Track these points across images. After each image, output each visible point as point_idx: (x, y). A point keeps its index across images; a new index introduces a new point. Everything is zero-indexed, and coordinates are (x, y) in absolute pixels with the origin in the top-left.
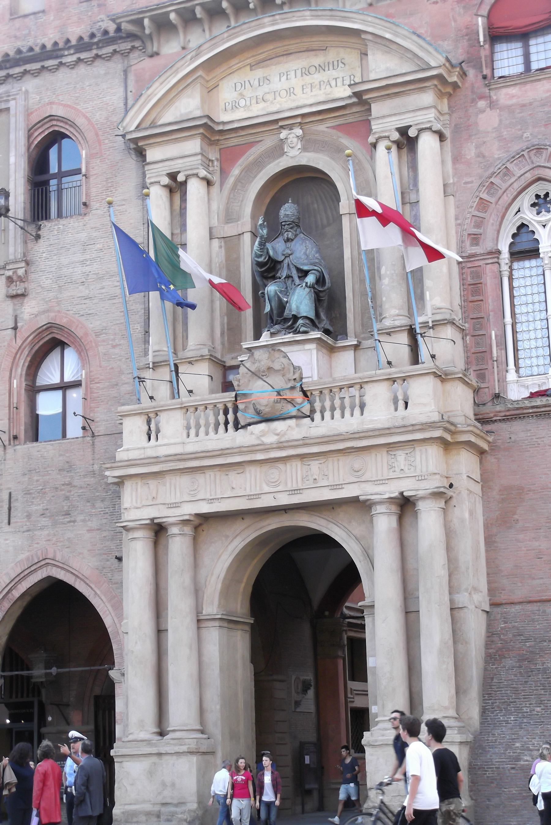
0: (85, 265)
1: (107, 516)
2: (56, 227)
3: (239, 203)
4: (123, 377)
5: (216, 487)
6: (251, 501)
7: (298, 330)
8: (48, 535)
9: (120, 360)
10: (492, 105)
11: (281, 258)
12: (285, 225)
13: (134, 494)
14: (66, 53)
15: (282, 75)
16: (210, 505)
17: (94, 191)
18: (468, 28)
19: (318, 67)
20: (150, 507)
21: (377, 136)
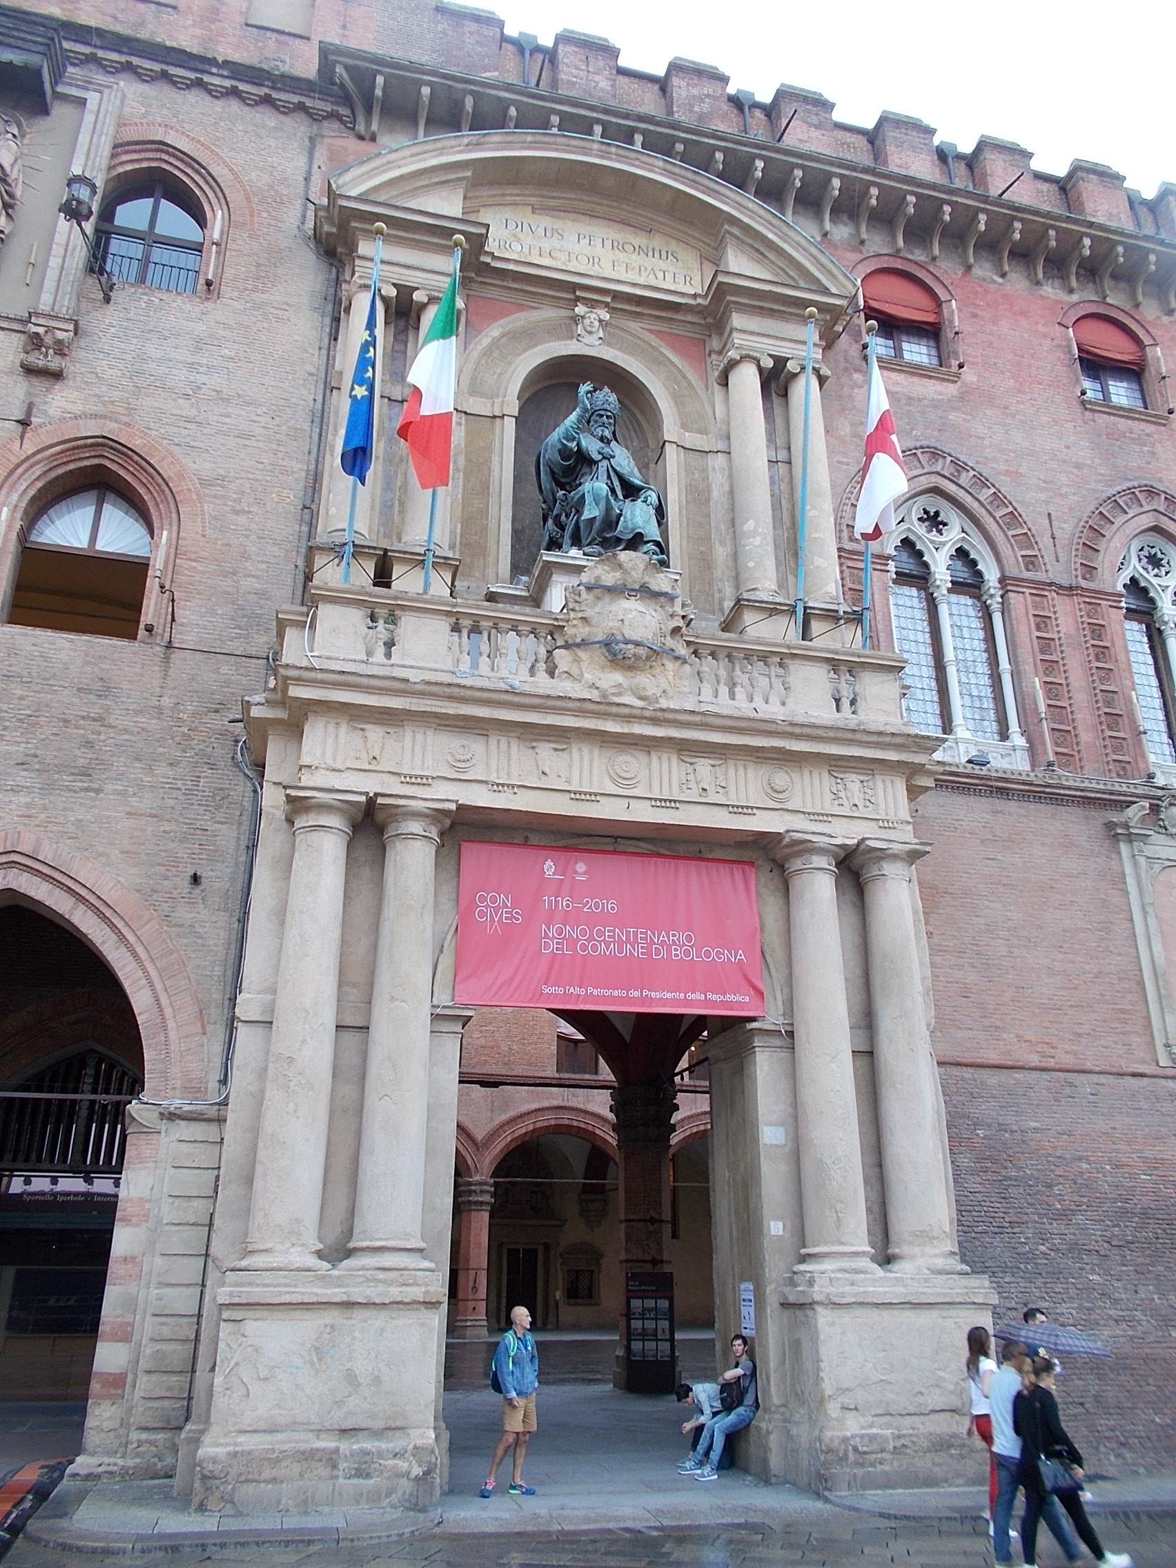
1: (175, 793)
2: (146, 298)
4: (248, 564)
5: (509, 765)
6: (580, 803)
8: (28, 805)
9: (247, 536)
13: (330, 741)
14: (214, 70)
17: (229, 273)
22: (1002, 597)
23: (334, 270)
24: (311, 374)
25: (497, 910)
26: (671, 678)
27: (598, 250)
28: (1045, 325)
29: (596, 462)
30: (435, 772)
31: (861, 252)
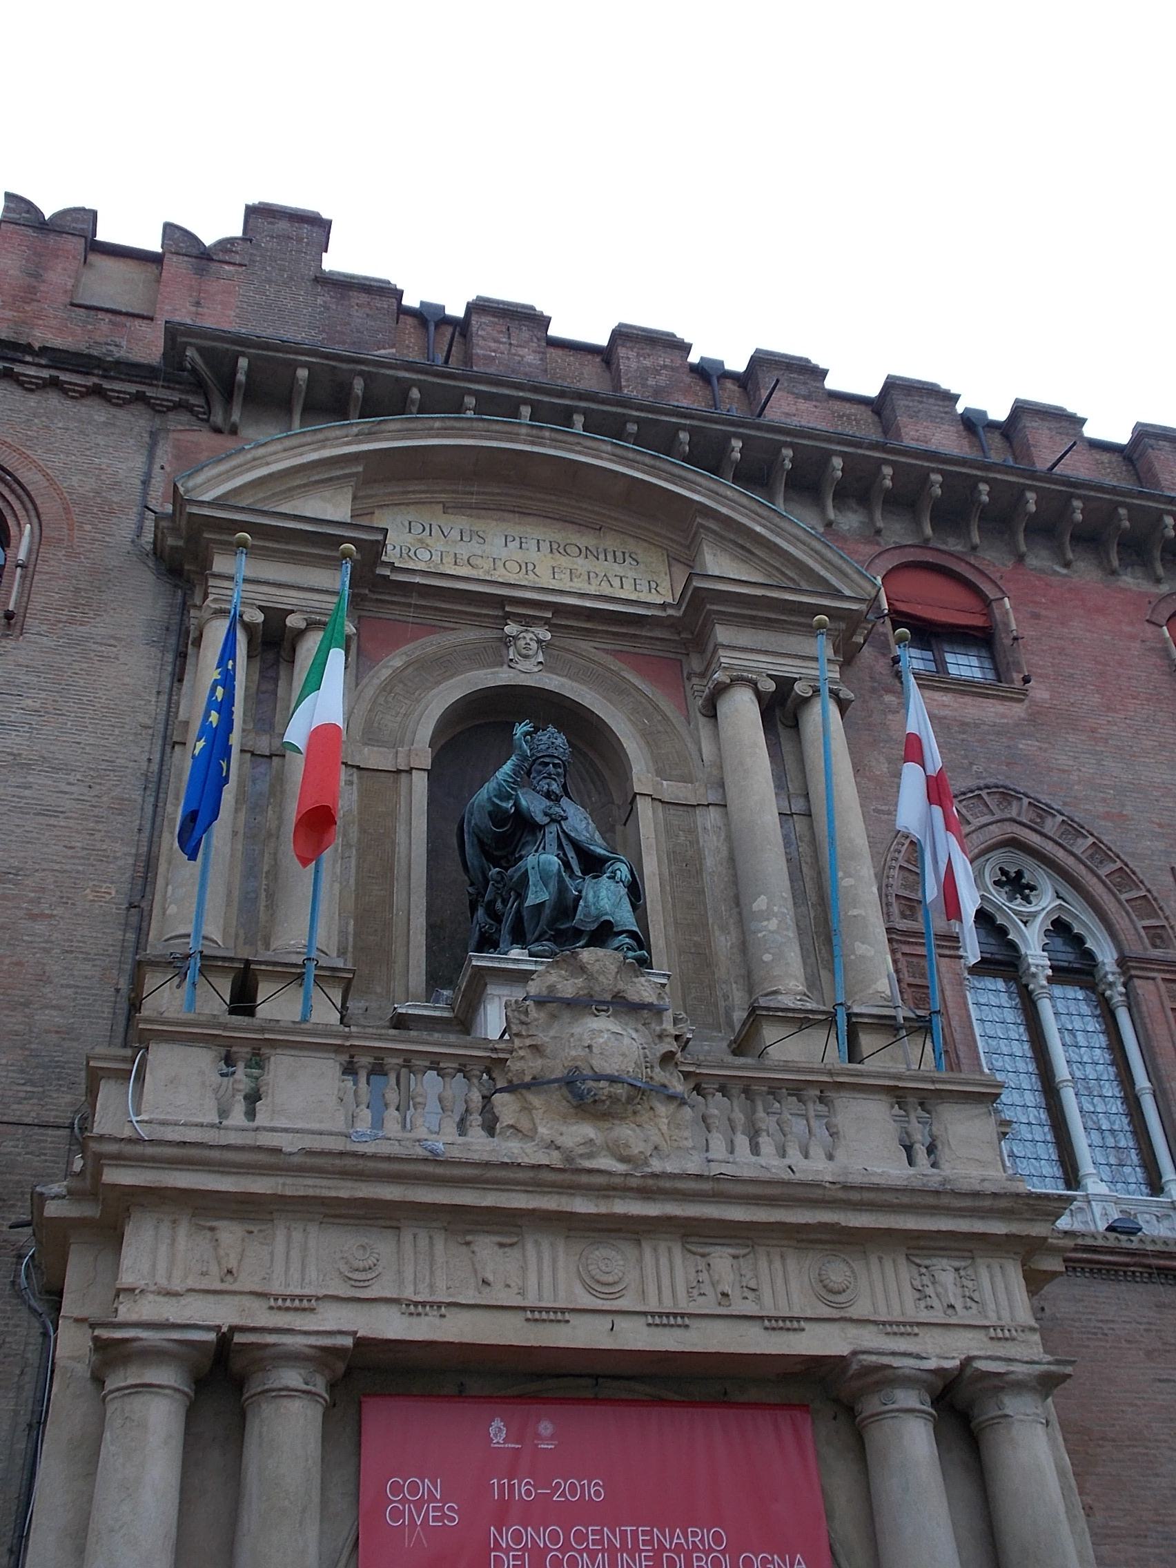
3: (399, 719)
4: (47, 990)
5: (432, 1273)
6: (541, 1326)
11: (541, 819)
12: (547, 764)
13: (163, 1249)
14: (28, 359)
15: (509, 539)
16: (415, 1320)
17: (38, 601)
19: (584, 550)
20: (211, 1298)
22: (1125, 985)
24: (146, 727)
25: (419, 1505)
26: (664, 1128)
27: (533, 555)
28: (1131, 623)
31: (878, 544)
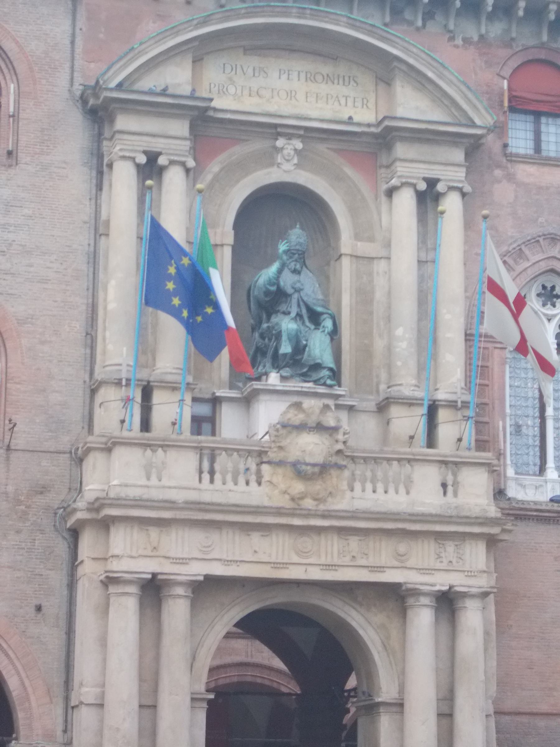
0: (7, 231)
7: (322, 381)
10: (510, 177)
11: (290, 291)
15: (282, 72)
17: (23, 140)
18: (489, 86)
20: (148, 559)
21: (404, 180)
23: (96, 126)
24: (85, 223)
29: (290, 295)
30: (190, 556)
31: (511, 47)
